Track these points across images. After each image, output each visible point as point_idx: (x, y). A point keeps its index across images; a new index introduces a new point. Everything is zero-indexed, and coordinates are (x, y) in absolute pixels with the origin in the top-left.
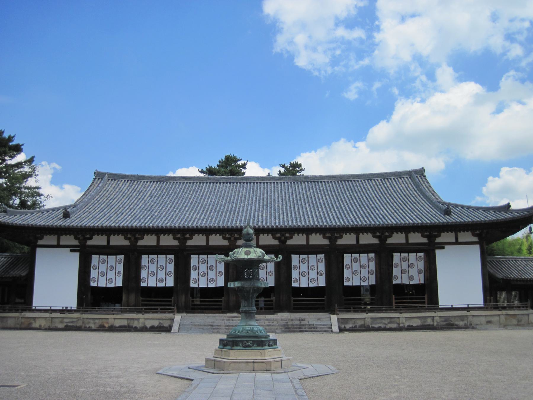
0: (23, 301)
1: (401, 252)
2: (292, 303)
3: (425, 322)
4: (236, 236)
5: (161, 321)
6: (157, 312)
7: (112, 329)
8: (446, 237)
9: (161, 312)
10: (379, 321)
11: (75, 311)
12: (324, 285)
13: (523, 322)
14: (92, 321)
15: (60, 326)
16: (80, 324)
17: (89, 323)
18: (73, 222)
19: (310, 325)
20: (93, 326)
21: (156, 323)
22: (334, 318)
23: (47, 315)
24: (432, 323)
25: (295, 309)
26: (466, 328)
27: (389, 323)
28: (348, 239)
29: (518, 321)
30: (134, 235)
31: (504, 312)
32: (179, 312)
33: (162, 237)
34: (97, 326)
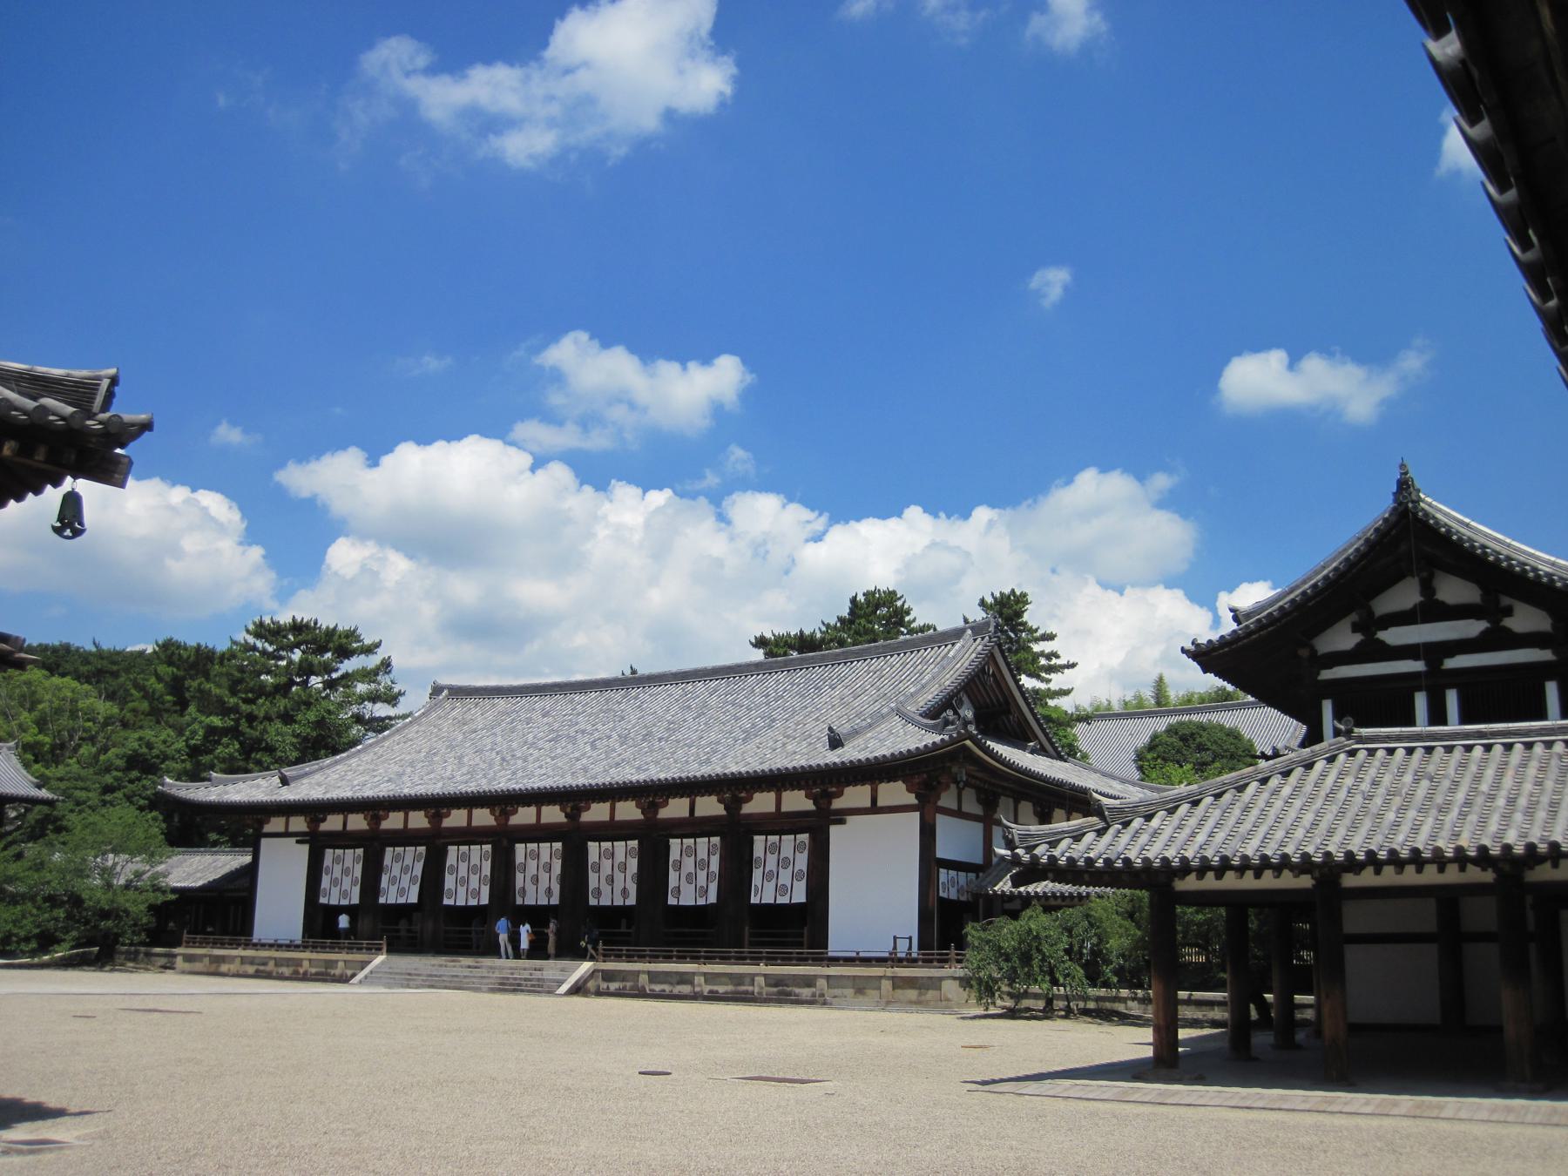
1: (767, 833)
8: (856, 796)
11: (297, 946)
12: (803, 899)
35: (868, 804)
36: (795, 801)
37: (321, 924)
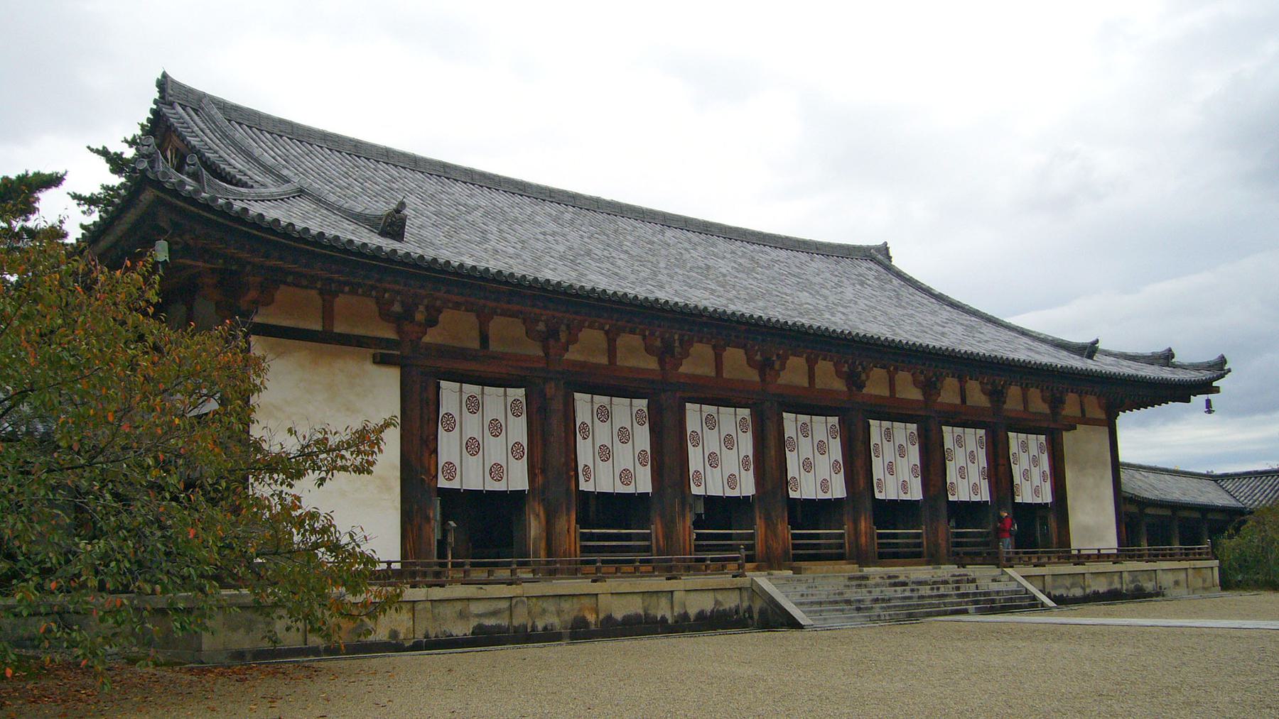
14: (551, 606)
15: (461, 629)
16: (520, 619)
17: (544, 611)
20: (554, 621)
21: (705, 603)
24: (1119, 586)
25: (882, 556)
26: (1157, 594)
34: (568, 618)
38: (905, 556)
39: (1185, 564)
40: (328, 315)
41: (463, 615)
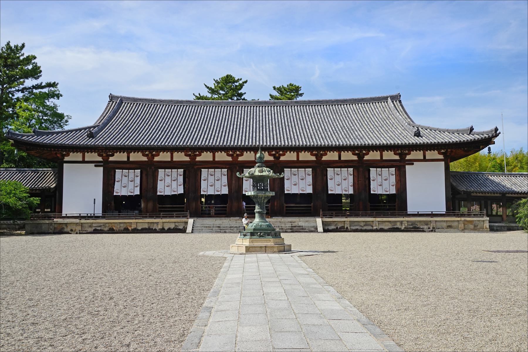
0: (49, 210)
2: (285, 208)
3: (394, 225)
4: (238, 153)
5: (177, 224)
6: (172, 217)
7: (135, 231)
9: (177, 217)
10: (356, 224)
13: (478, 227)
18: (99, 141)
19: (299, 226)
21: (172, 226)
22: (319, 221)
23: (77, 221)
24: (400, 227)
25: (287, 213)
27: (364, 226)
28: (332, 156)
29: (475, 226)
30: (151, 153)
31: (463, 219)
32: (191, 217)
33: (175, 154)
35: (422, 158)
36: (389, 155)
37: (114, 205)
38: (299, 213)
39: (459, 219)
40: (84, 157)
41: (90, 226)
